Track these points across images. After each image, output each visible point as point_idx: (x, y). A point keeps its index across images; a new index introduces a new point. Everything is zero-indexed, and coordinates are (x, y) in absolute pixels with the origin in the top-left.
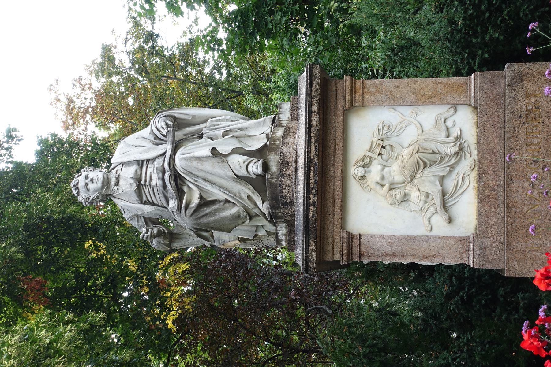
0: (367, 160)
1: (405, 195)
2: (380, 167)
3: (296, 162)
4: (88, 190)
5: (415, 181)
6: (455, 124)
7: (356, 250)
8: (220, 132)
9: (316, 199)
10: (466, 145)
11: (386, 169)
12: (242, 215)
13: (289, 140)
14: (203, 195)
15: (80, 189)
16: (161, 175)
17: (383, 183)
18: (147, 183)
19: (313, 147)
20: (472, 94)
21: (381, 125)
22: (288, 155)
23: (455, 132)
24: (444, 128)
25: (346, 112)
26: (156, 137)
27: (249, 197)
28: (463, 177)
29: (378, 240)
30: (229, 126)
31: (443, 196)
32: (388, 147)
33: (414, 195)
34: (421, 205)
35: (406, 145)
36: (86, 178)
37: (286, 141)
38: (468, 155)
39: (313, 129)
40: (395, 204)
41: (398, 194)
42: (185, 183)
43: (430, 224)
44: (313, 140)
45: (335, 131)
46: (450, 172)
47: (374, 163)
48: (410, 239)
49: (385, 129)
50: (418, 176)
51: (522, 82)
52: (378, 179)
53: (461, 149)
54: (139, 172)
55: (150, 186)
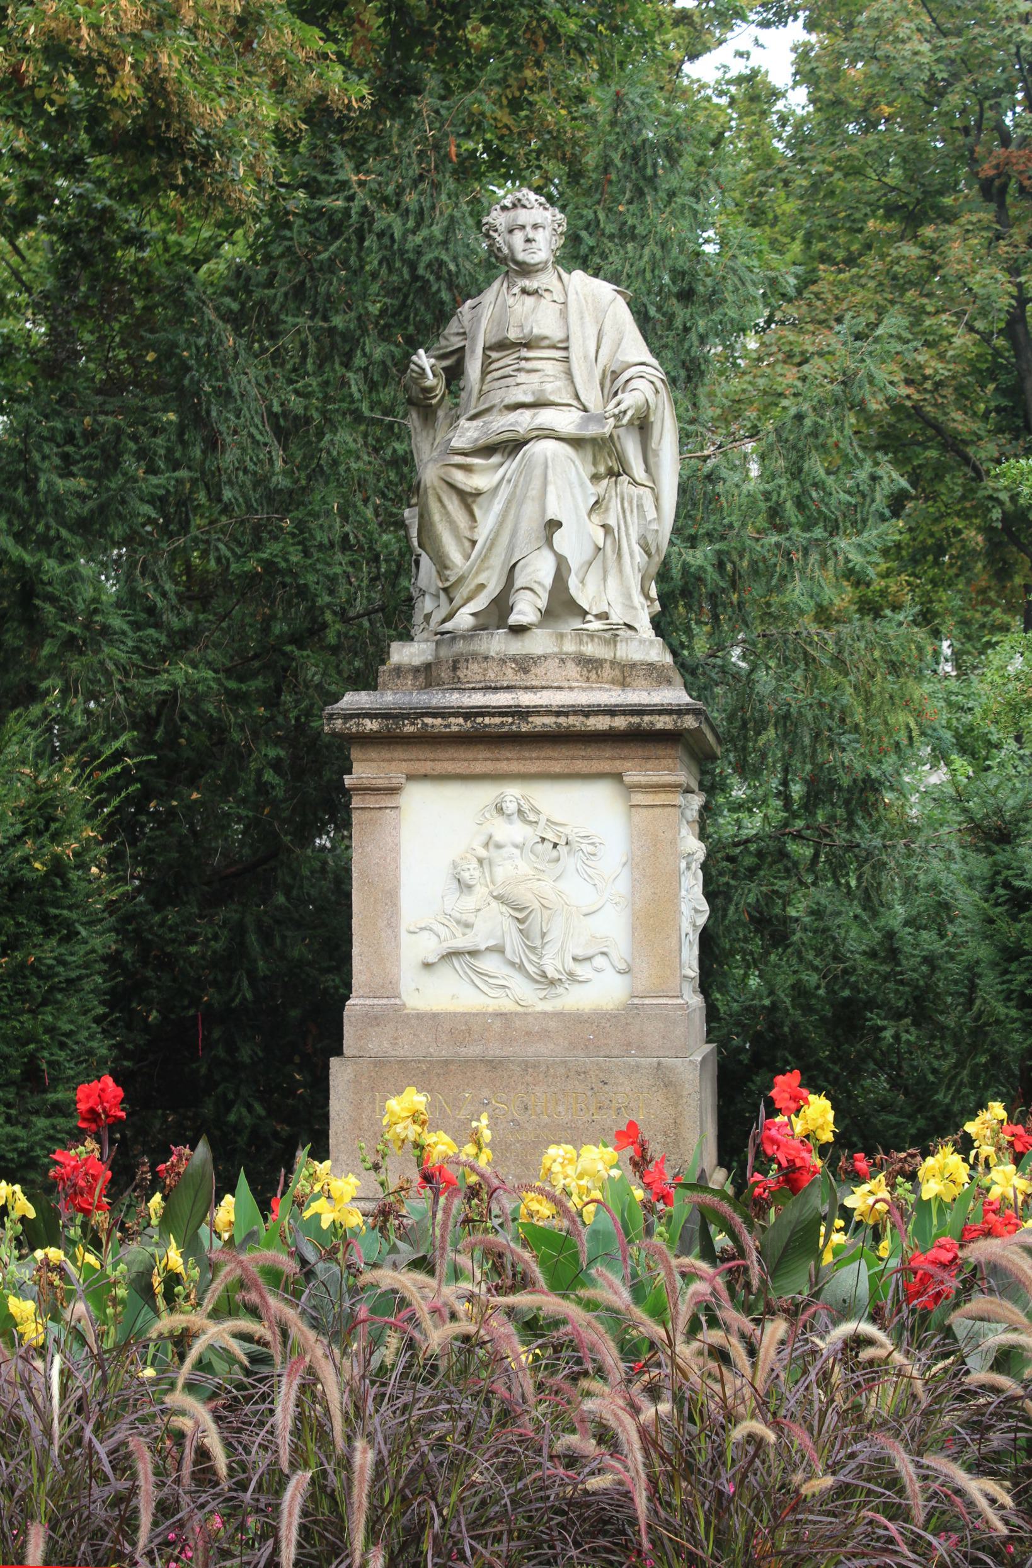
0: (532, 817)
1: (470, 887)
2: (519, 840)
3: (526, 688)
4: (511, 231)
5: (495, 904)
6: (597, 970)
7: (371, 801)
8: (612, 522)
9: (455, 729)
10: (560, 990)
11: (517, 852)
12: (448, 572)
13: (572, 670)
14: (480, 499)
15: (512, 213)
16: (529, 399)
17: (491, 847)
18: (523, 364)
19: (549, 720)
20: (647, 1001)
21: (596, 840)
22: (539, 670)
23: (582, 971)
24: (590, 953)
25: (618, 777)
26: (615, 375)
27: (482, 587)
28: (504, 987)
29: (389, 840)
30: (628, 535)
31: (469, 953)
32: (555, 853)
33: (470, 902)
34: (453, 913)
35: (560, 885)
36: (535, 227)
37: (570, 665)
38: (543, 994)
39: (581, 718)
40: (455, 867)
41: (471, 873)
42: (510, 454)
43: (421, 929)
44: (562, 720)
45: (583, 758)
46: (513, 964)
47: (528, 830)
48: (391, 897)
49: (590, 849)
50: (504, 908)
51: (666, 1086)
52: (498, 838)
53: (552, 983)
54: (546, 343)
55: (518, 370)
